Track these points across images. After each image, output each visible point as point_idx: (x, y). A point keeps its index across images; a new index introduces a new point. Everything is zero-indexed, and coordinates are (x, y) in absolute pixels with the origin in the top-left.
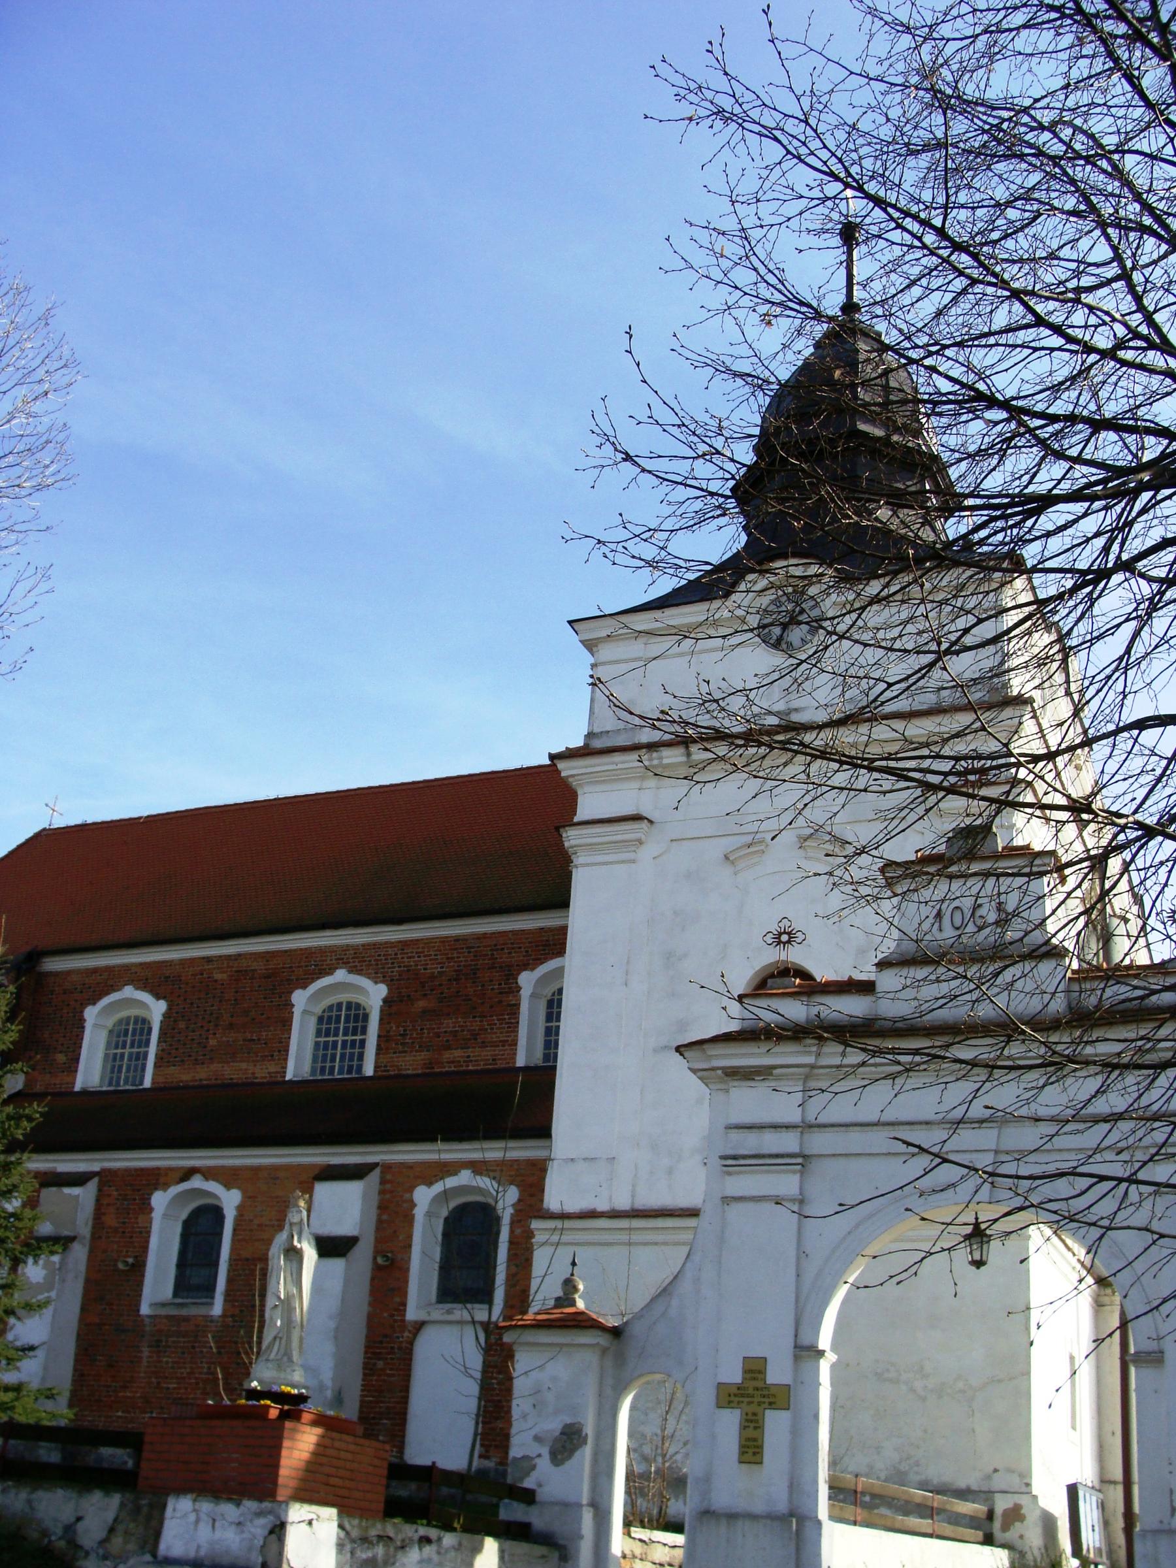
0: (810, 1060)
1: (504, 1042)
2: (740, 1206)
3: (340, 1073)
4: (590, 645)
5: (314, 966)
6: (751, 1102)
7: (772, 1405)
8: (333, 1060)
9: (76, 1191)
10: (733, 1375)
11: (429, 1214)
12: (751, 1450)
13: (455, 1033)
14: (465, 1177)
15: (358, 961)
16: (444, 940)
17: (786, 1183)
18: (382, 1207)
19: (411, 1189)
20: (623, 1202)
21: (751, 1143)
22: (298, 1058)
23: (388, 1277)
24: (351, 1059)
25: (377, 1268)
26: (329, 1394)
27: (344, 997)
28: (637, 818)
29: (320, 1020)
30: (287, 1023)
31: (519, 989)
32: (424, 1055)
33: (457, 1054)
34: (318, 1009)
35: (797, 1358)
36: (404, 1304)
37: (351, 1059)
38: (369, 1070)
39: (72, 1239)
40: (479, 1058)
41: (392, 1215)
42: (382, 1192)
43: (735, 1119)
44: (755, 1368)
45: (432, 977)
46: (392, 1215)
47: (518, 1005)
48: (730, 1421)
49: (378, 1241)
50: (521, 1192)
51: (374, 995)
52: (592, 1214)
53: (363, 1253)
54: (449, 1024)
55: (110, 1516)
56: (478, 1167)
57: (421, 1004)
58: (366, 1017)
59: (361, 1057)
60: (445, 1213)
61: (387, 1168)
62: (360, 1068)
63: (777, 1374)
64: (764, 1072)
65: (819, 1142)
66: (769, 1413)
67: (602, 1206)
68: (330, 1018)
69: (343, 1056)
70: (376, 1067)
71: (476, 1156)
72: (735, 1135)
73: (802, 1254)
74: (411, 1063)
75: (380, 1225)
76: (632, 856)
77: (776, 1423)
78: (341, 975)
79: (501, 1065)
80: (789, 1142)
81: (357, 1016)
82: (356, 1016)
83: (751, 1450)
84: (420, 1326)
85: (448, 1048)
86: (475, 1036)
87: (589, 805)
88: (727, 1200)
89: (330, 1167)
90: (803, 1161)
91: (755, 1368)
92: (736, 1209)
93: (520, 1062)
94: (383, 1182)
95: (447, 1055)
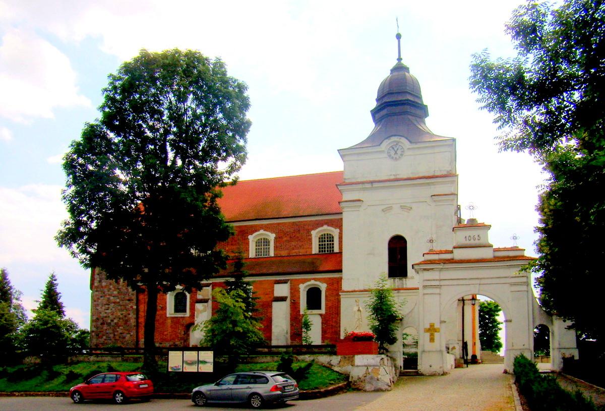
0: (441, 267)
2: (427, 296)
3: (264, 255)
4: (342, 156)
5: (254, 229)
6: (428, 275)
7: (436, 332)
8: (261, 252)
9: (207, 288)
10: (428, 326)
11: (304, 290)
12: (432, 340)
13: (295, 246)
14: (313, 282)
15: (266, 228)
16: (289, 223)
17: (437, 291)
18: (291, 289)
19: (298, 285)
20: (362, 289)
21: (429, 283)
22: (252, 253)
23: (295, 306)
25: (291, 303)
27: (262, 237)
28: (359, 200)
29: (256, 243)
30: (248, 244)
31: (311, 235)
32: (286, 251)
33: (297, 251)
34: (256, 240)
35: (440, 323)
38: (272, 254)
39: (209, 299)
40: (302, 251)
41: (294, 291)
42: (291, 286)
43: (425, 279)
44: (432, 326)
45: (287, 232)
46: (294, 291)
48: (428, 335)
50: (327, 284)
51: (272, 237)
52: (355, 291)
53: (288, 300)
54: (293, 243)
55: (339, 360)
56: (315, 279)
57: (285, 239)
58: (269, 242)
59: (269, 251)
60: (307, 290)
61: (292, 280)
62: (269, 255)
63: (436, 326)
64: (432, 269)
65: (442, 283)
66: (435, 333)
67: (356, 289)
69: (264, 251)
72: (426, 282)
73: (440, 304)
75: (291, 293)
76: (358, 209)
77: (436, 335)
78: (262, 231)
79: (308, 253)
80: (437, 283)
81: (267, 242)
82: (266, 242)
83: (432, 340)
85: (293, 249)
86: (300, 246)
87: (346, 197)
88: (424, 294)
89: (276, 280)
90: (439, 286)
91: (432, 326)
92: (426, 296)
93: (313, 253)
94: (291, 283)
95: (294, 251)
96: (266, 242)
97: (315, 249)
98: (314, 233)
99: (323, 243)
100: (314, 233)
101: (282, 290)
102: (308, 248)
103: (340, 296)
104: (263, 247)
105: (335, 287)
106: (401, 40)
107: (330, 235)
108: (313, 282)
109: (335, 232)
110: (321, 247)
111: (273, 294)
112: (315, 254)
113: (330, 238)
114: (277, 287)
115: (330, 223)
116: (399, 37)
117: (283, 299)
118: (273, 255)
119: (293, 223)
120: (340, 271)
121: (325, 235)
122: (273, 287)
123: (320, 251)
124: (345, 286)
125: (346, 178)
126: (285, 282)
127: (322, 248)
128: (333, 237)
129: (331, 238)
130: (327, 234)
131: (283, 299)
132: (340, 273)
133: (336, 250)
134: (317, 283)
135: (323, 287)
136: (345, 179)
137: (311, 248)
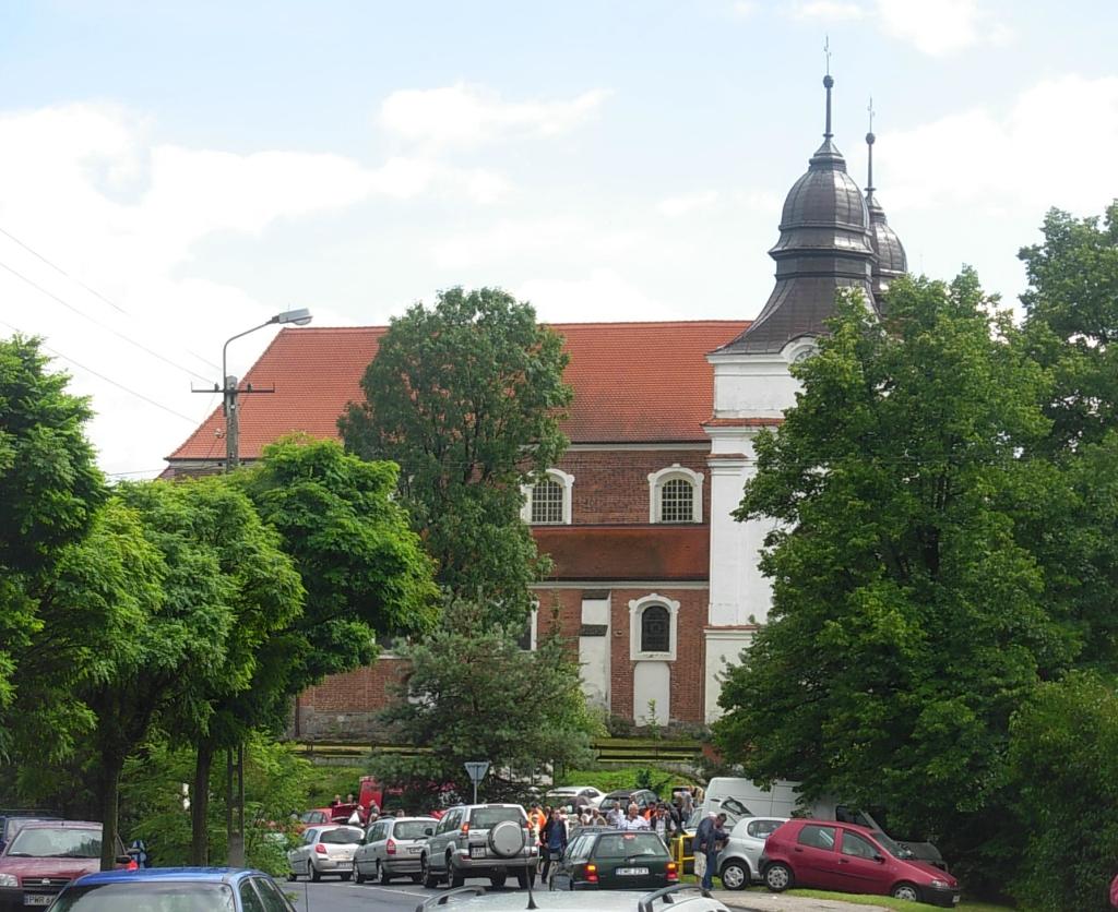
1: (642, 510)
8: (544, 513)
11: (637, 613)
14: (653, 597)
24: (555, 511)
26: (604, 696)
31: (648, 482)
33: (617, 514)
36: (629, 653)
37: (555, 511)
38: (567, 519)
40: (630, 517)
41: (620, 615)
46: (620, 615)
47: (648, 491)
49: (612, 625)
52: (730, 628)
54: (610, 499)
56: (659, 592)
57: (595, 487)
59: (560, 512)
60: (643, 610)
61: (615, 591)
67: (734, 624)
68: (540, 490)
70: (573, 519)
71: (658, 587)
74: (593, 518)
84: (637, 662)
87: (718, 447)
93: (652, 521)
95: (611, 516)
96: (555, 491)
97: (655, 514)
98: (653, 478)
99: (672, 500)
100: (653, 478)
101: (596, 612)
102: (642, 510)
103: (705, 635)
104: (547, 501)
105: (697, 605)
106: (832, 90)
107: (686, 483)
108: (653, 597)
109: (697, 479)
110: (667, 509)
111: (580, 617)
112: (655, 524)
113: (685, 489)
114: (587, 606)
115: (687, 460)
116: (828, 82)
117: (598, 631)
118: (569, 522)
119: (612, 453)
120: (705, 578)
121: (674, 482)
122: (581, 604)
123: (664, 518)
124: (715, 619)
125: (719, 409)
126: (601, 596)
127: (669, 510)
128: (691, 489)
129: (686, 489)
130: (680, 482)
131: (598, 631)
132: (705, 583)
133: (698, 517)
134: (661, 599)
135: (674, 607)
136: (716, 411)
137: (648, 511)
